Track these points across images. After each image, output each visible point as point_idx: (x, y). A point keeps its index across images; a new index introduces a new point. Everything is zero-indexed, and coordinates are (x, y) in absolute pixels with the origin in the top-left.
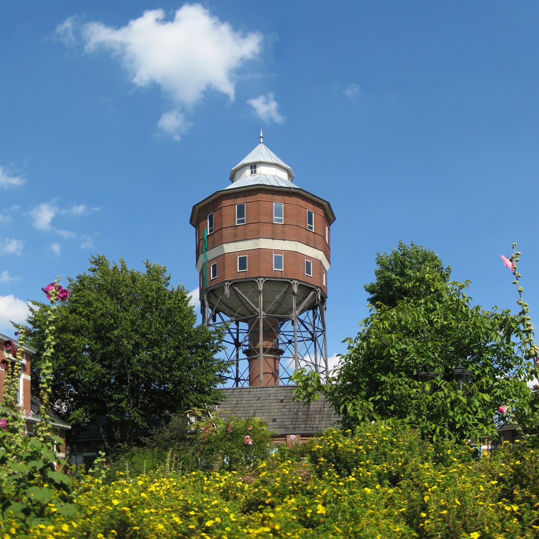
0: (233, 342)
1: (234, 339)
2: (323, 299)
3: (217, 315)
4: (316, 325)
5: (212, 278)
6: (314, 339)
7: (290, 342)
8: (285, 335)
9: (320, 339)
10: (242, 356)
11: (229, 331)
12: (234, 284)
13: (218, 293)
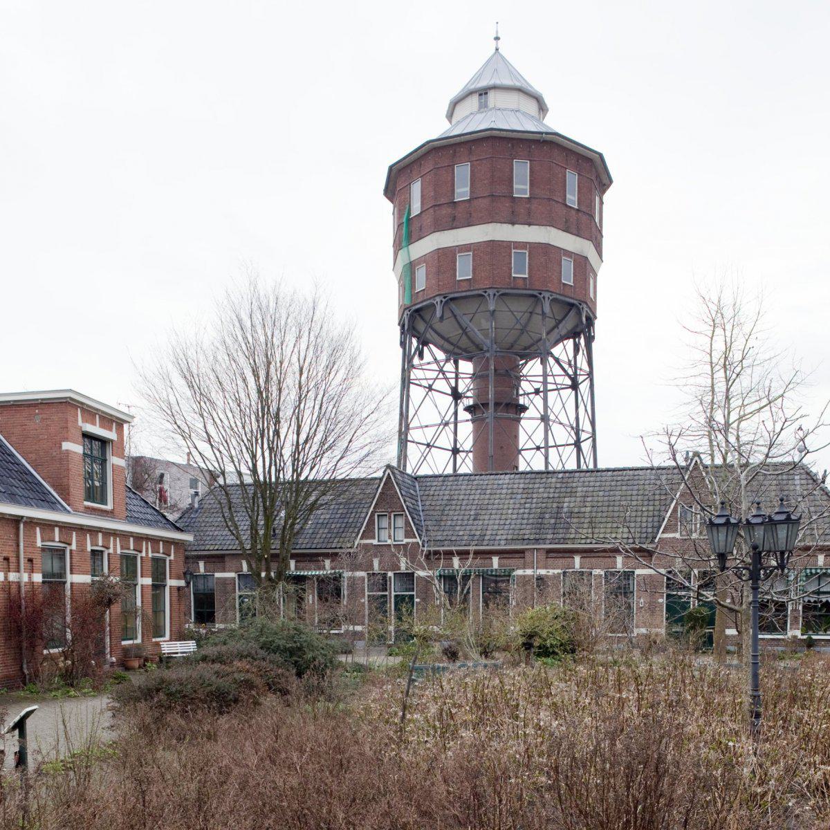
0: (450, 392)
2: (590, 321)
3: (425, 348)
4: (579, 365)
6: (575, 386)
7: (537, 392)
9: (584, 387)
10: (464, 415)
11: (444, 374)
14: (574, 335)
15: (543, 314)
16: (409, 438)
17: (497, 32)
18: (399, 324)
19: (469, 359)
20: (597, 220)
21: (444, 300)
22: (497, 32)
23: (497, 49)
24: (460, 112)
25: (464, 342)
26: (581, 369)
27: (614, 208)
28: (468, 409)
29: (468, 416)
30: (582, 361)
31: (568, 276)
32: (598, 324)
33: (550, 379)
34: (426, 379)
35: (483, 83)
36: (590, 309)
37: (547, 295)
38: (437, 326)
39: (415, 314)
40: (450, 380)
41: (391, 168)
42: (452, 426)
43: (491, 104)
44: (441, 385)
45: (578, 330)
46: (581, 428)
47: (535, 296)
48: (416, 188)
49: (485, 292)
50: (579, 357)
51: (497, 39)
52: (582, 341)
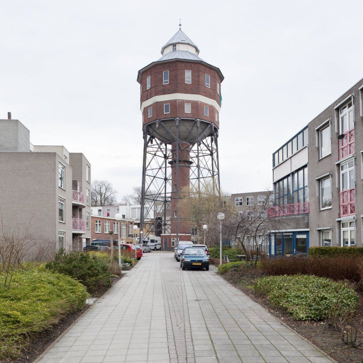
0: (163, 156)
1: (164, 155)
2: (216, 130)
3: (153, 139)
5: (149, 117)
6: (212, 154)
8: (194, 152)
9: (215, 155)
10: (168, 165)
11: (161, 149)
12: (162, 121)
13: (153, 127)
15: (197, 127)
16: (146, 174)
17: (180, 23)
18: (143, 130)
19: (170, 144)
22: (180, 23)
23: (180, 29)
24: (167, 51)
25: (168, 137)
27: (225, 88)
28: (170, 163)
29: (170, 165)
31: (207, 114)
34: (154, 151)
35: (174, 42)
37: (199, 120)
38: (157, 131)
39: (149, 127)
40: (163, 152)
41: (139, 72)
42: (164, 170)
43: (177, 49)
44: (159, 153)
47: (194, 120)
48: (149, 79)
49: (175, 119)
51: (180, 25)
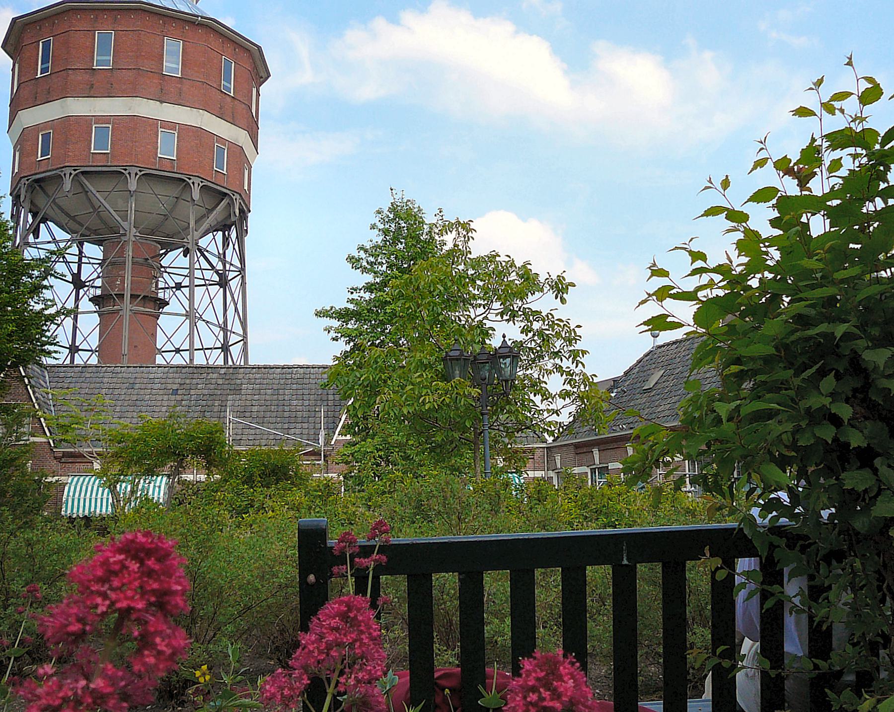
2: (244, 214)
4: (228, 259)
6: (223, 283)
9: (234, 284)
12: (83, 173)
13: (50, 190)
14: (224, 227)
19: (99, 243)
20: (254, 111)
21: (73, 172)
26: (231, 264)
28: (94, 300)
29: (92, 307)
30: (231, 255)
32: (252, 219)
33: (198, 274)
36: (244, 201)
45: (228, 223)
46: (229, 328)
50: (229, 252)
52: (234, 235)
